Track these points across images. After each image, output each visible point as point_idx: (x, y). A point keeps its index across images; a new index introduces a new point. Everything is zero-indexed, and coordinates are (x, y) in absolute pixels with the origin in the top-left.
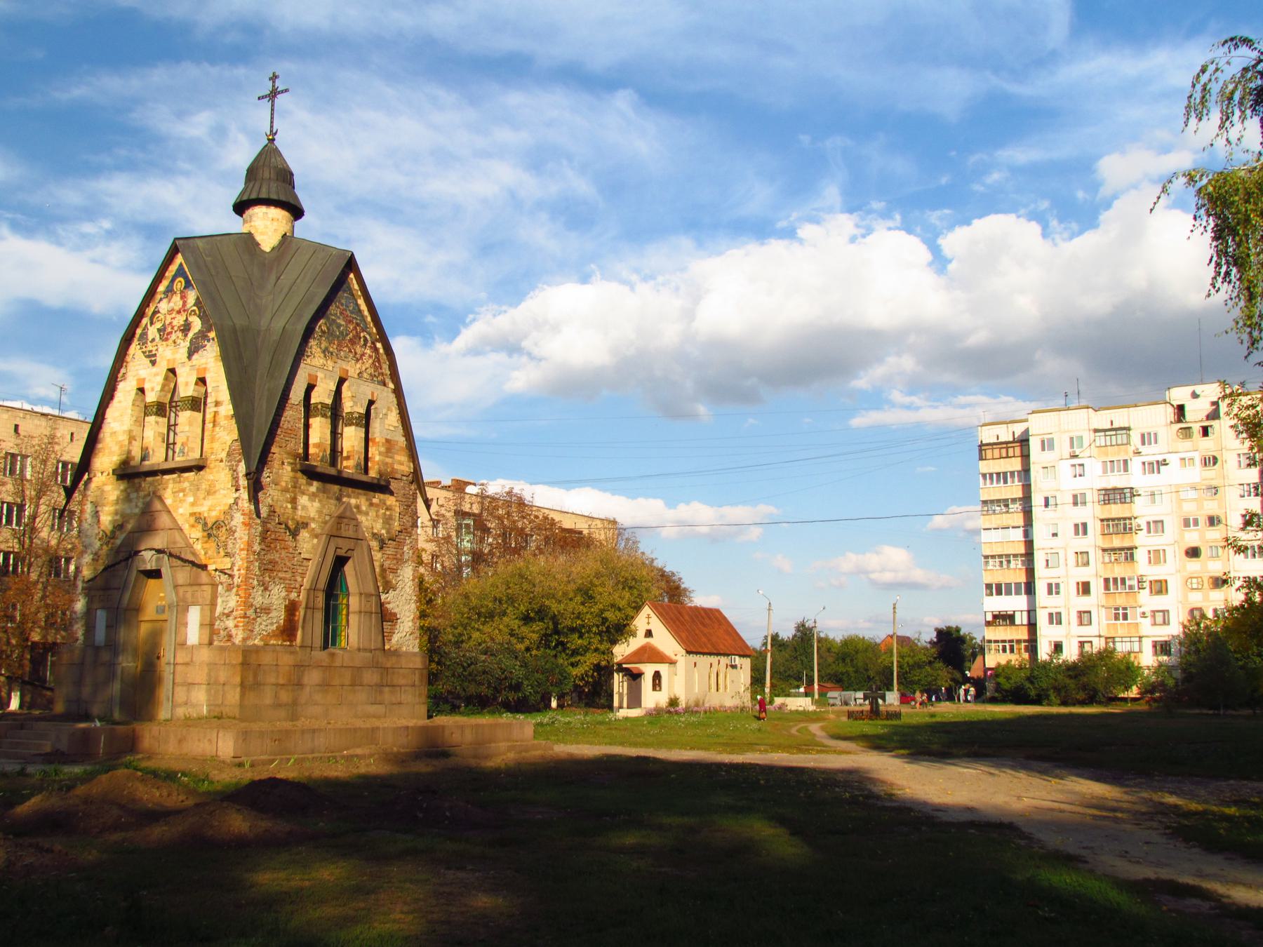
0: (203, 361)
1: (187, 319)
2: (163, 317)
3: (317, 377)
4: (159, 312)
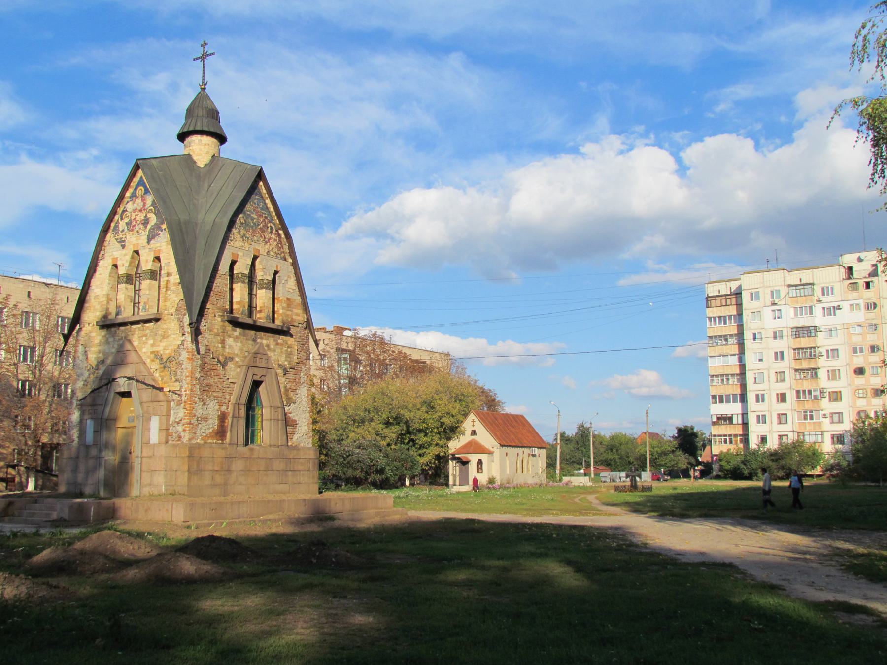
0: (158, 245)
1: (146, 215)
2: (129, 214)
3: (238, 255)
4: (126, 211)
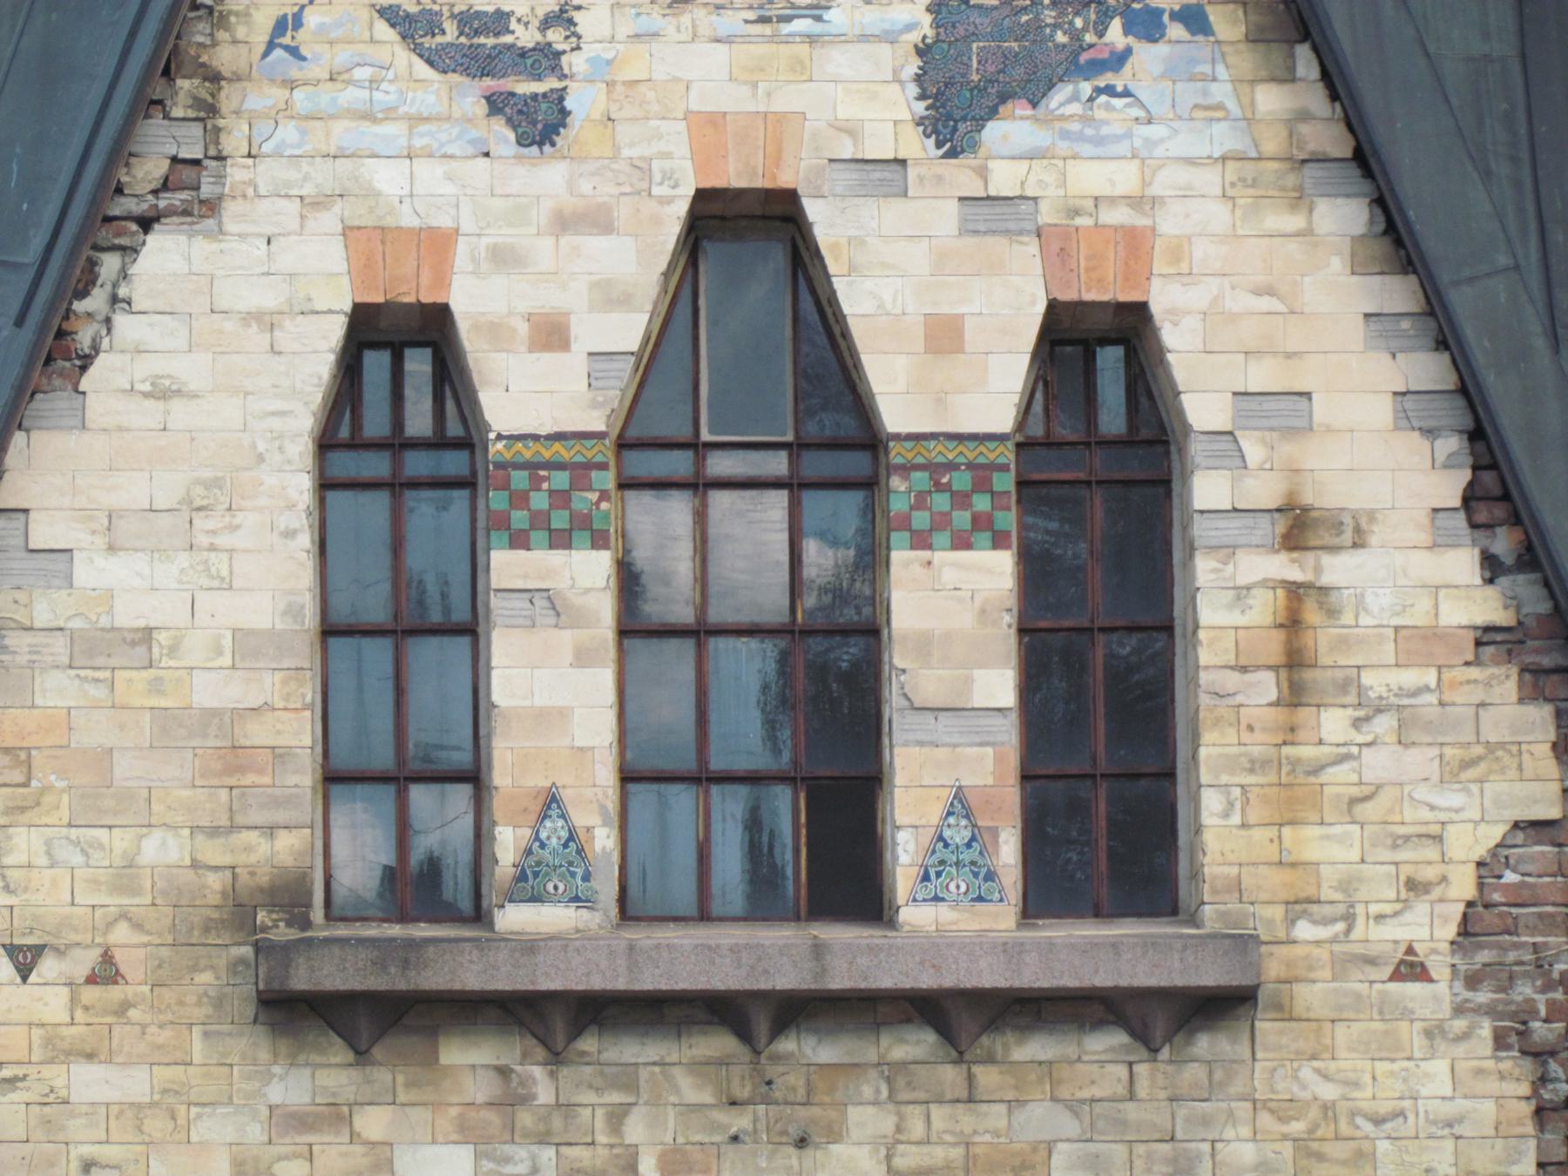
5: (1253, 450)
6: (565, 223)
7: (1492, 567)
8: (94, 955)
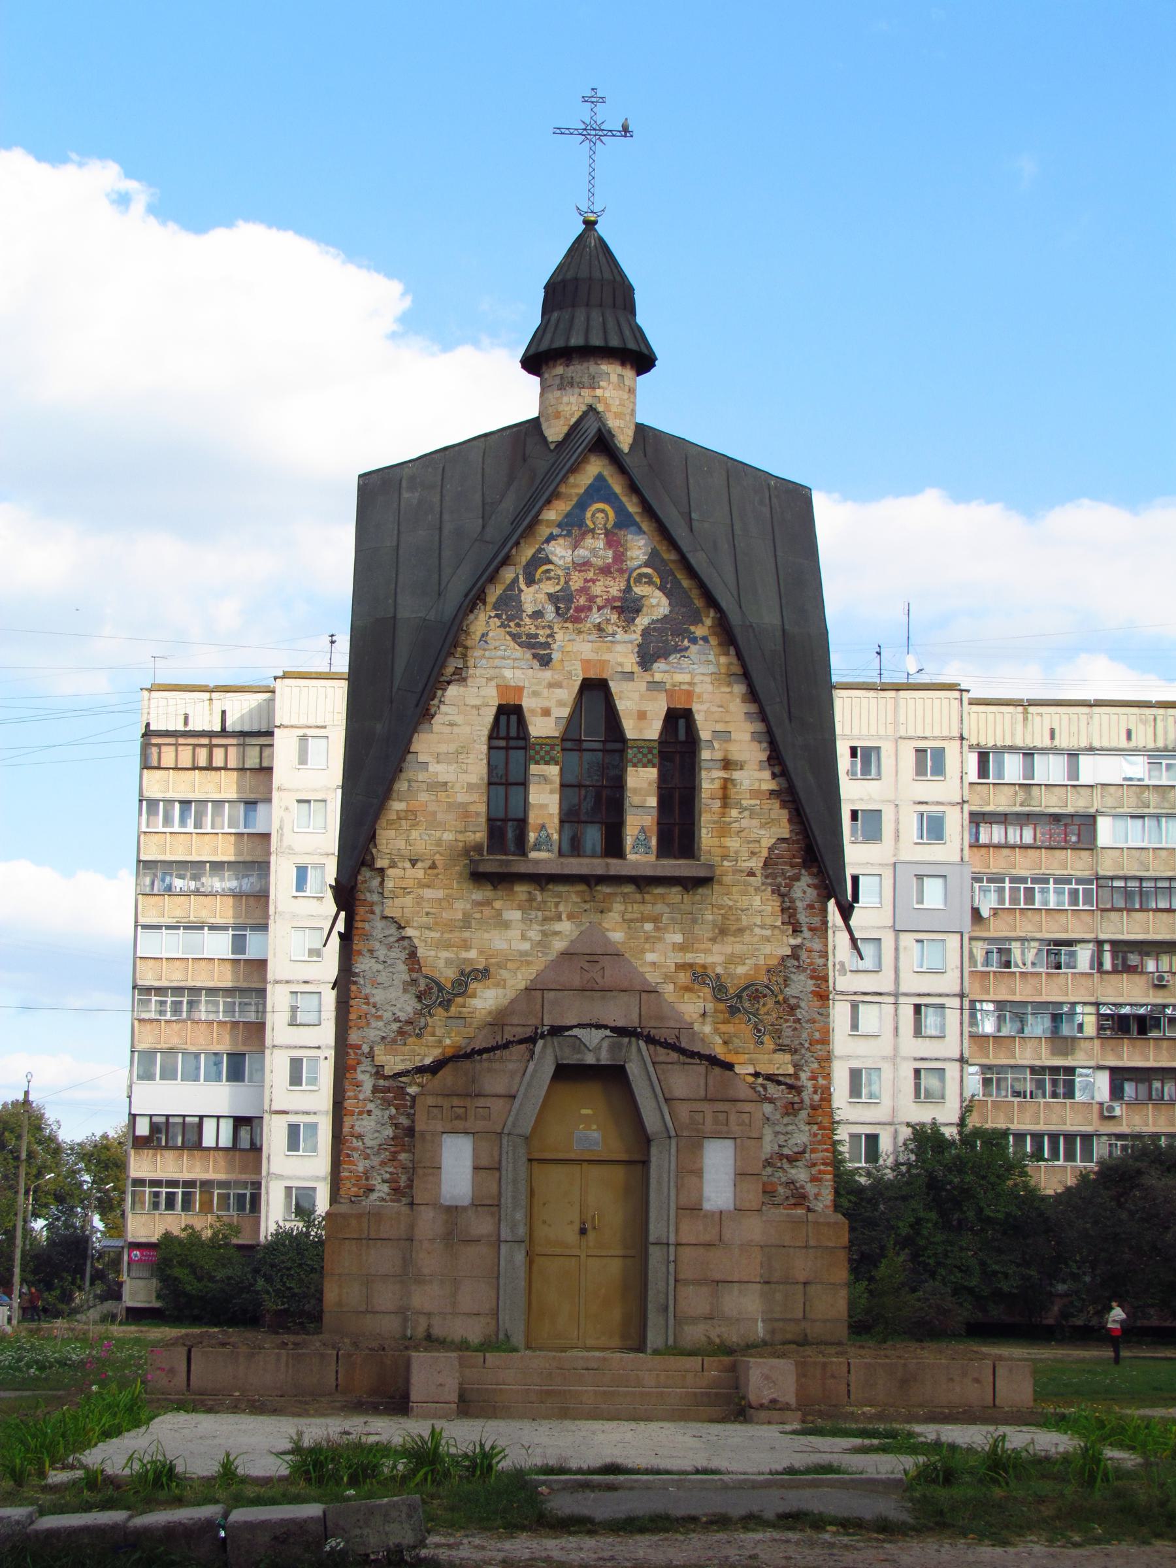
0: (679, 677)
1: (628, 589)
5: (716, 745)
6: (551, 685)
7: (774, 776)
8: (431, 862)
